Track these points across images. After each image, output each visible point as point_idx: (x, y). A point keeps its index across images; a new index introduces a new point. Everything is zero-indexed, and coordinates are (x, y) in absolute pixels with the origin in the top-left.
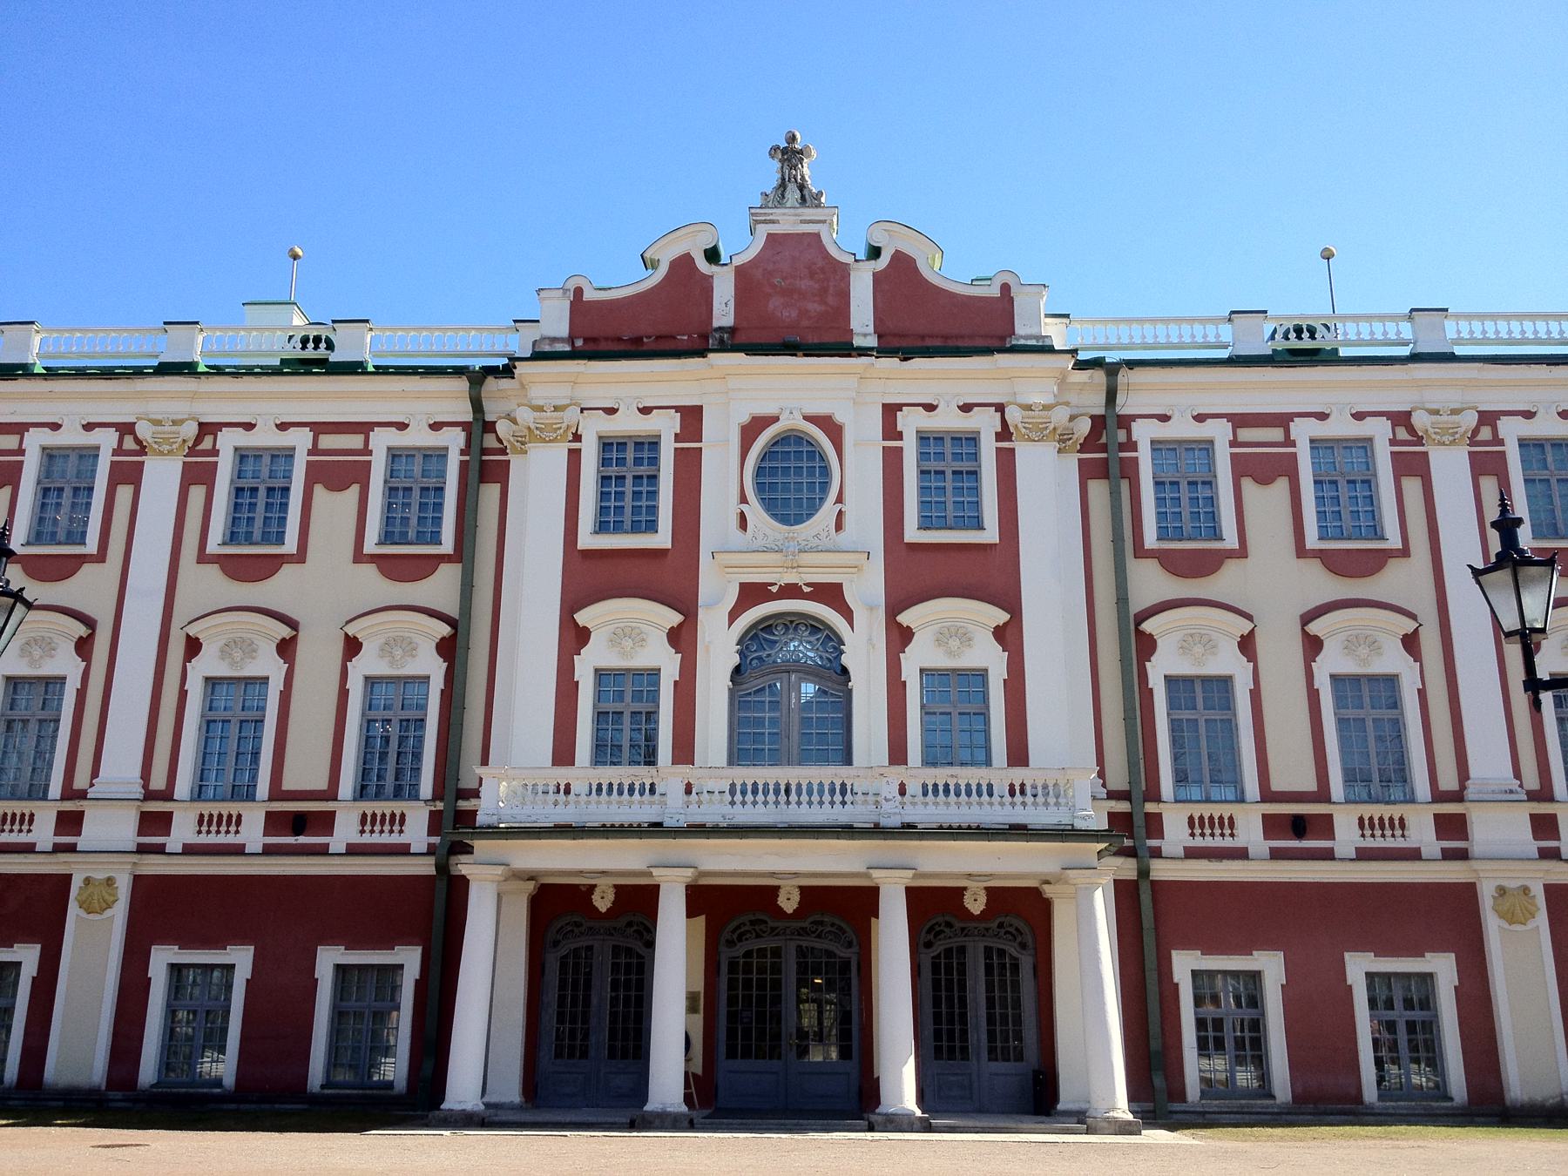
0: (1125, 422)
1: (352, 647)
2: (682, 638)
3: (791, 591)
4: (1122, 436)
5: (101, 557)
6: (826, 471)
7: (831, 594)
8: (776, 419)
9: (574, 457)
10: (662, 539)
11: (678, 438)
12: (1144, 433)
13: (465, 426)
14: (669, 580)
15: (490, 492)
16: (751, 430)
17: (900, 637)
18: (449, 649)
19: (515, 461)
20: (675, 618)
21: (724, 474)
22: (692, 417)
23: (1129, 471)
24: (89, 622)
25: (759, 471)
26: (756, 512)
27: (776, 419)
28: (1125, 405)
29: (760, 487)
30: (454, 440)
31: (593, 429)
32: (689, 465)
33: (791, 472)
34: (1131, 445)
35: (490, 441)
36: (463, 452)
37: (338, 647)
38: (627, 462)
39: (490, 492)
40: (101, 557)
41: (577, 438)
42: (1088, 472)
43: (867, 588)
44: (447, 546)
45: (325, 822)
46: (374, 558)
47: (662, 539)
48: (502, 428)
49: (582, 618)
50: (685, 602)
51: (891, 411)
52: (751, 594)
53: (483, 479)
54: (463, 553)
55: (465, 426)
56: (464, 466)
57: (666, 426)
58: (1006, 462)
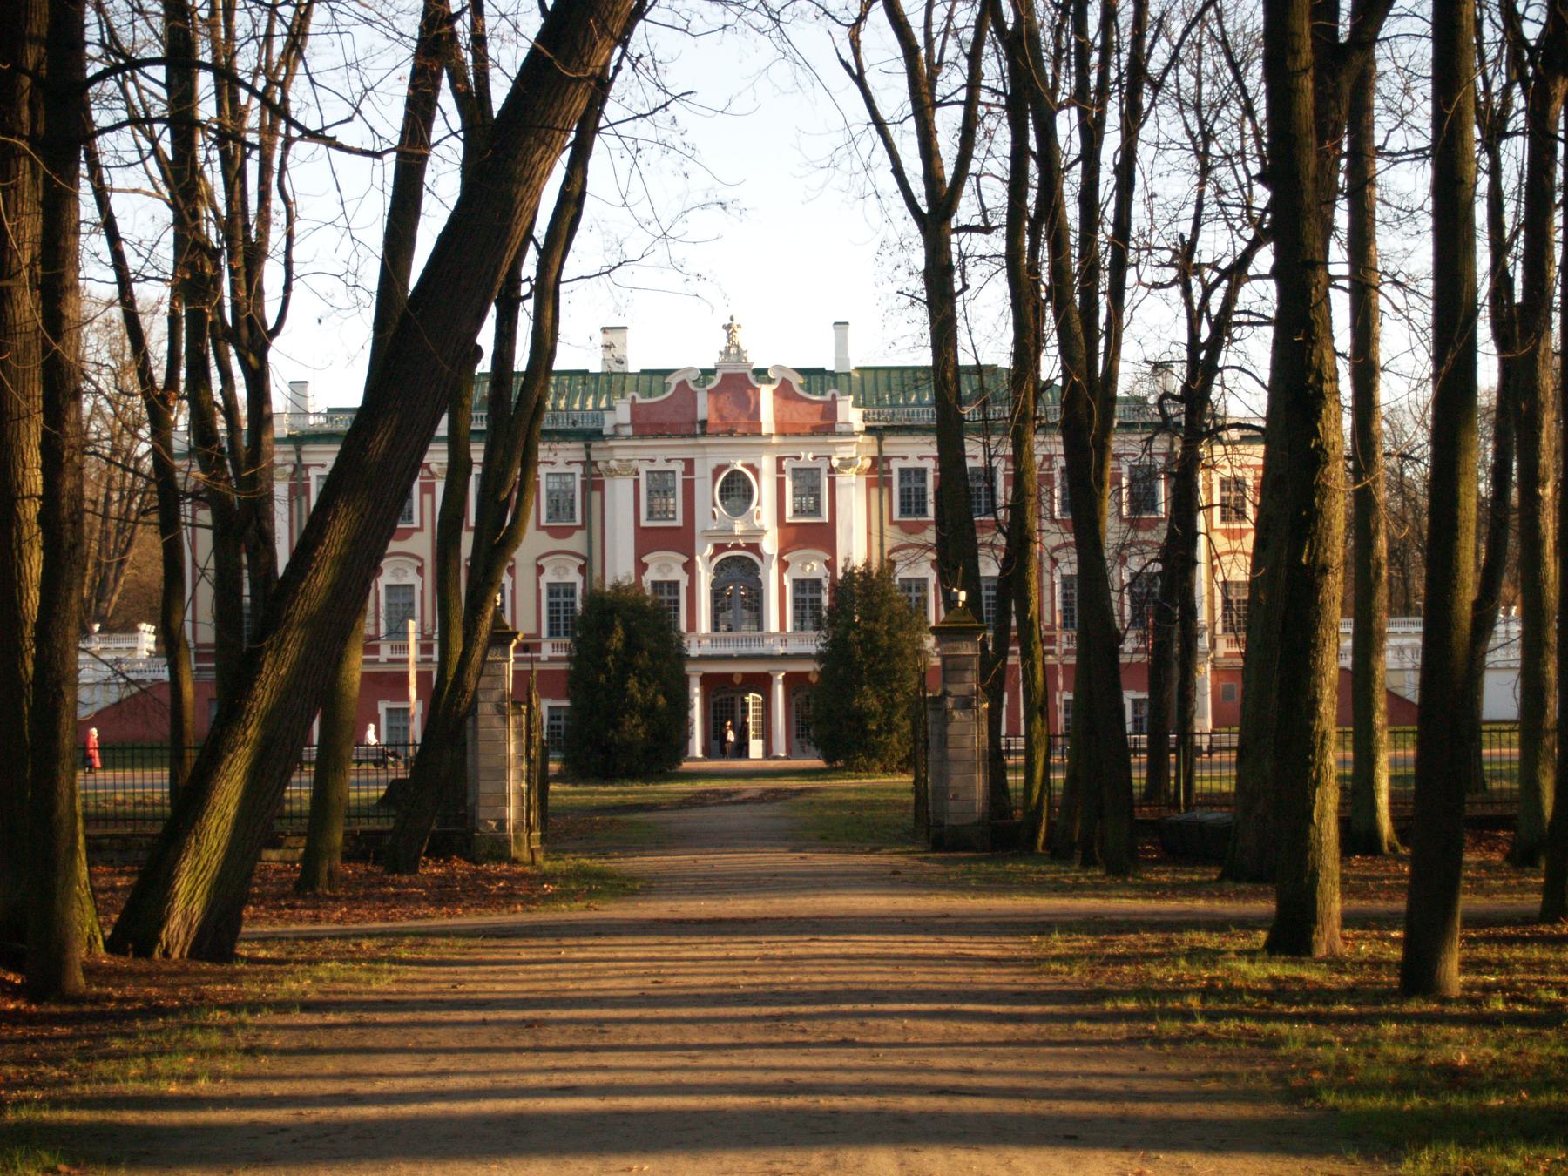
0: (887, 459)
1: (540, 570)
2: (690, 568)
3: (737, 547)
4: (885, 466)
5: (421, 529)
6: (750, 490)
7: (754, 548)
8: (727, 466)
9: (637, 482)
10: (679, 522)
11: (684, 474)
12: (896, 465)
13: (582, 463)
14: (682, 540)
15: (596, 496)
16: (717, 472)
17: (784, 566)
18: (582, 569)
19: (608, 483)
20: (685, 559)
21: (707, 492)
22: (690, 464)
23: (888, 483)
24: (421, 560)
25: (721, 490)
26: (720, 510)
27: (727, 466)
28: (887, 451)
29: (722, 498)
30: (578, 470)
31: (643, 469)
32: (689, 487)
33: (736, 490)
34: (890, 471)
35: (594, 471)
36: (583, 475)
37: (533, 571)
38: (660, 485)
39: (596, 496)
40: (421, 529)
41: (637, 473)
42: (870, 484)
43: (770, 544)
44: (578, 521)
45: (538, 648)
46: (544, 528)
47: (679, 522)
48: (601, 465)
49: (644, 559)
50: (690, 553)
51: (780, 460)
52: (719, 548)
53: (593, 489)
54: (586, 524)
55: (582, 463)
56: (583, 483)
57: (679, 468)
58: (832, 483)
